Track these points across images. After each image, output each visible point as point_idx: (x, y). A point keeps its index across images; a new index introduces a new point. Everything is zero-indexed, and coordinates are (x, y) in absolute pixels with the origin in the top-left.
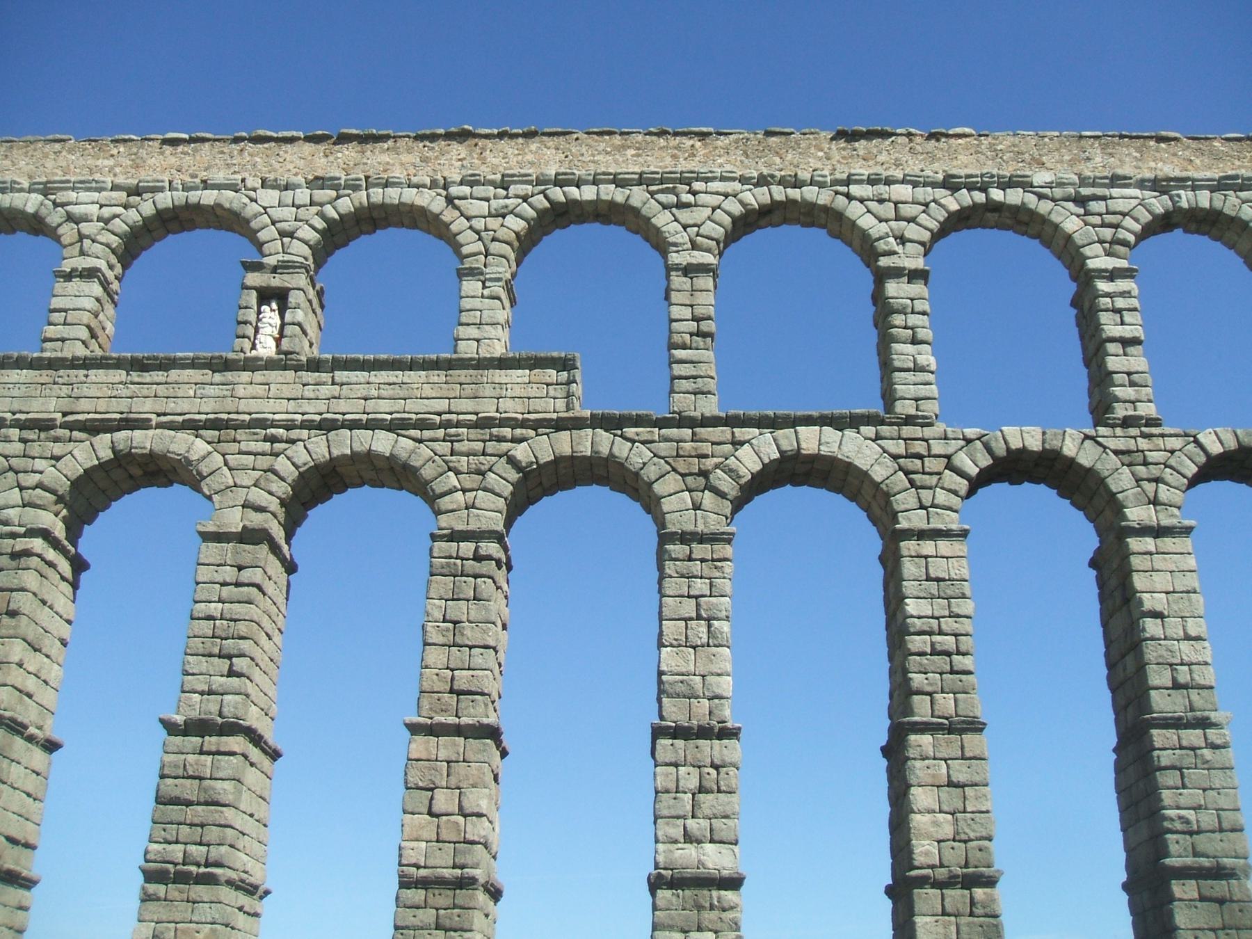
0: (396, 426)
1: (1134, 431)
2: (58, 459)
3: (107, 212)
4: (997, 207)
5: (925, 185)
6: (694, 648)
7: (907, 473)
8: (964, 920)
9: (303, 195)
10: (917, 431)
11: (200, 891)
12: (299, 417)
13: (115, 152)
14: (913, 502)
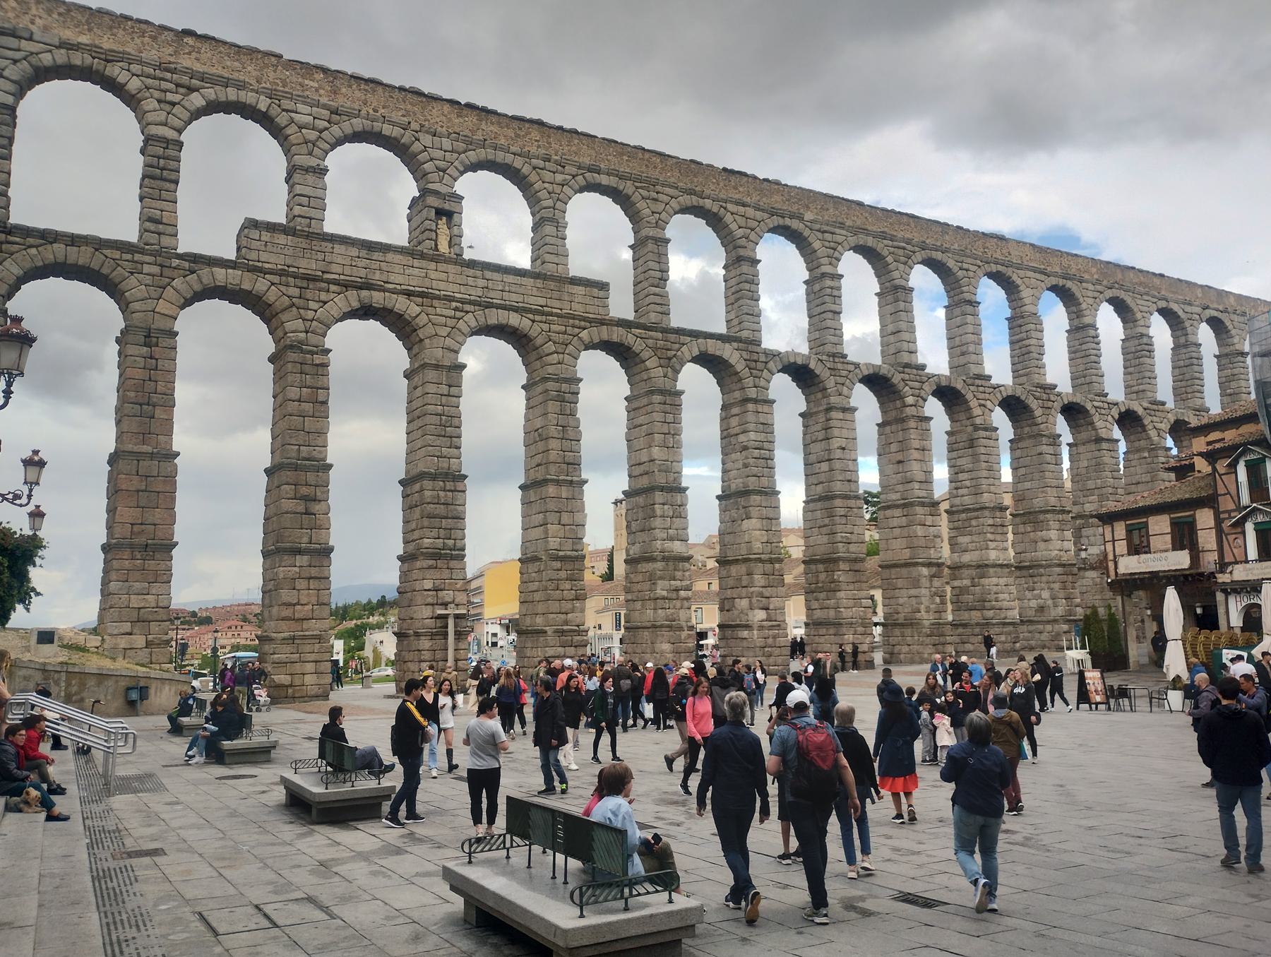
3: (322, 124)
5: (759, 210)
9: (446, 143)
11: (453, 564)
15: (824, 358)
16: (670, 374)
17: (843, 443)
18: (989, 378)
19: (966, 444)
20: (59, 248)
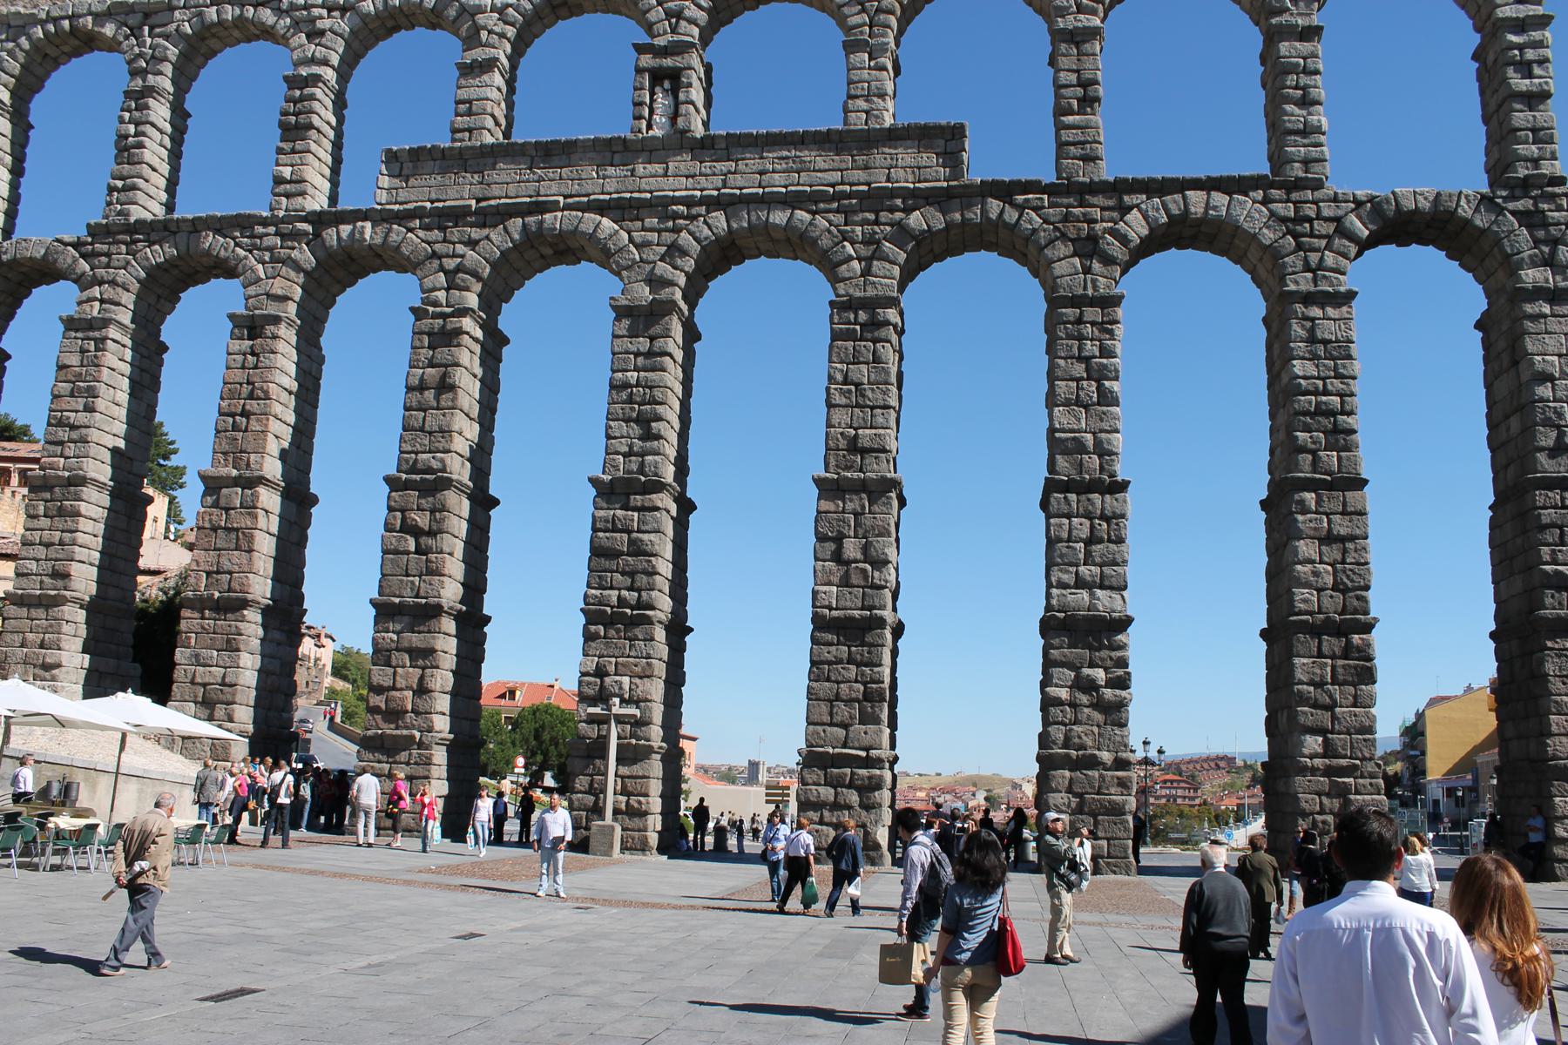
0: (791, 201)
2: (477, 242)
6: (1086, 407)
7: (1296, 236)
8: (1340, 662)
10: (1309, 194)
12: (698, 193)
14: (1300, 264)
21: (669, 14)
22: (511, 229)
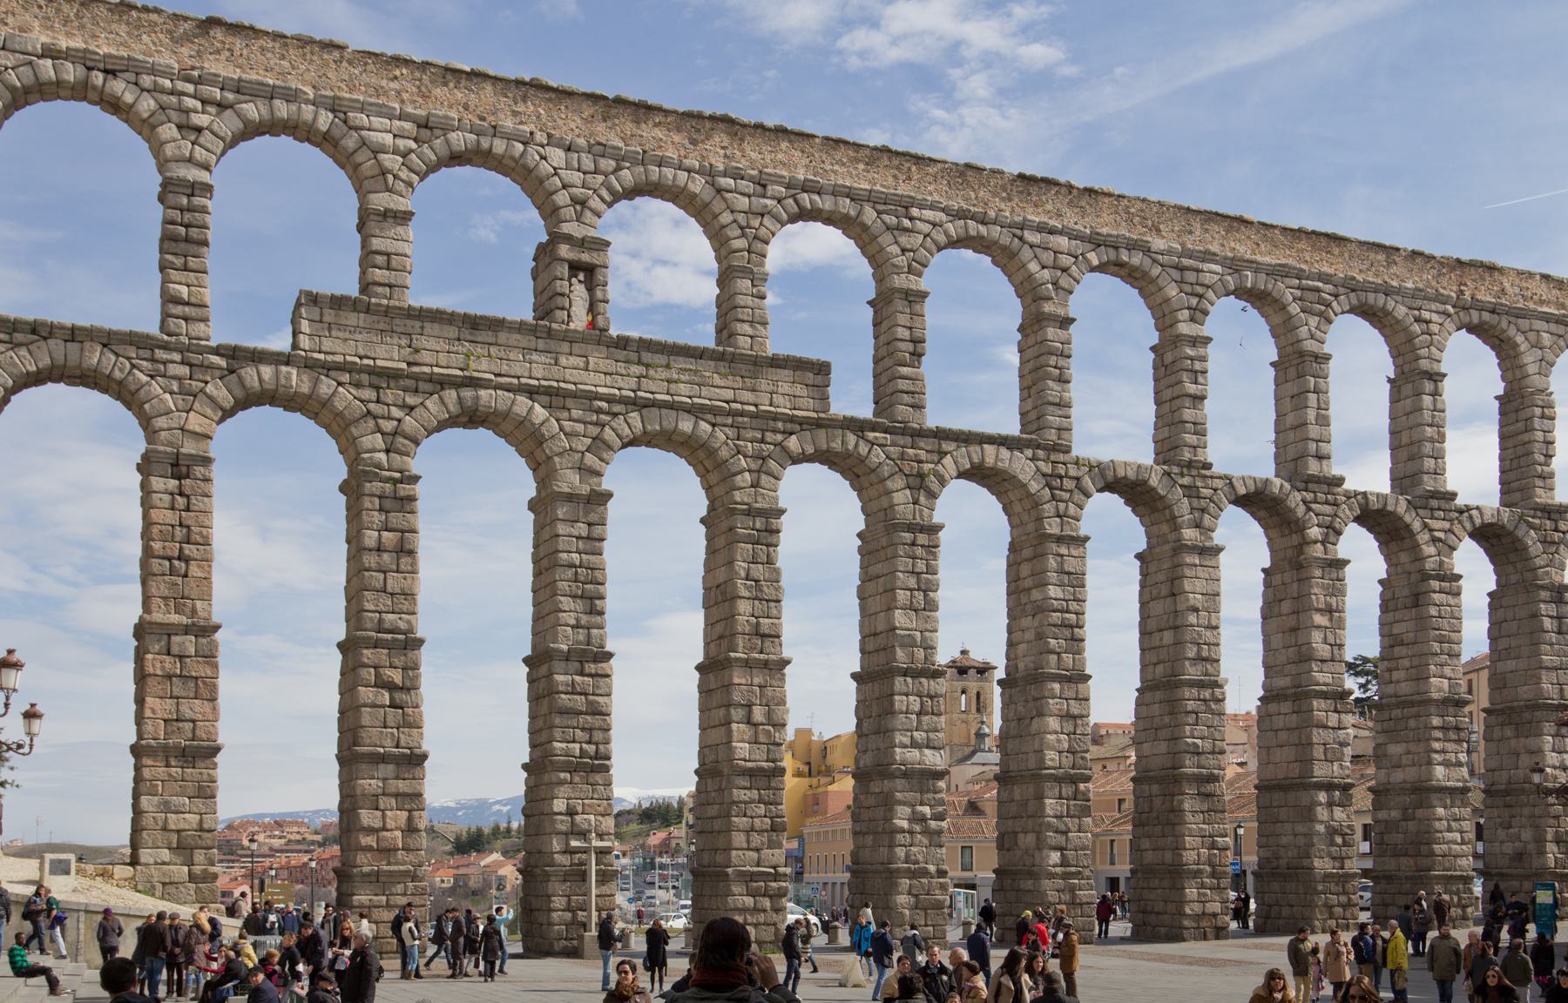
0: (696, 411)
1: (1194, 472)
2: (412, 408)
4: (1121, 264)
10: (1061, 457)
13: (397, 73)
14: (1053, 511)
15: (1176, 470)
16: (922, 499)
17: (1196, 599)
18: (1453, 495)
19: (1409, 602)
20: (56, 345)
21: (576, 201)
22: (447, 400)
